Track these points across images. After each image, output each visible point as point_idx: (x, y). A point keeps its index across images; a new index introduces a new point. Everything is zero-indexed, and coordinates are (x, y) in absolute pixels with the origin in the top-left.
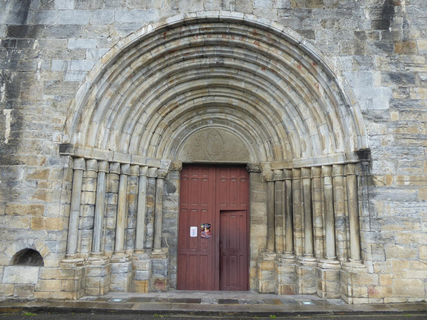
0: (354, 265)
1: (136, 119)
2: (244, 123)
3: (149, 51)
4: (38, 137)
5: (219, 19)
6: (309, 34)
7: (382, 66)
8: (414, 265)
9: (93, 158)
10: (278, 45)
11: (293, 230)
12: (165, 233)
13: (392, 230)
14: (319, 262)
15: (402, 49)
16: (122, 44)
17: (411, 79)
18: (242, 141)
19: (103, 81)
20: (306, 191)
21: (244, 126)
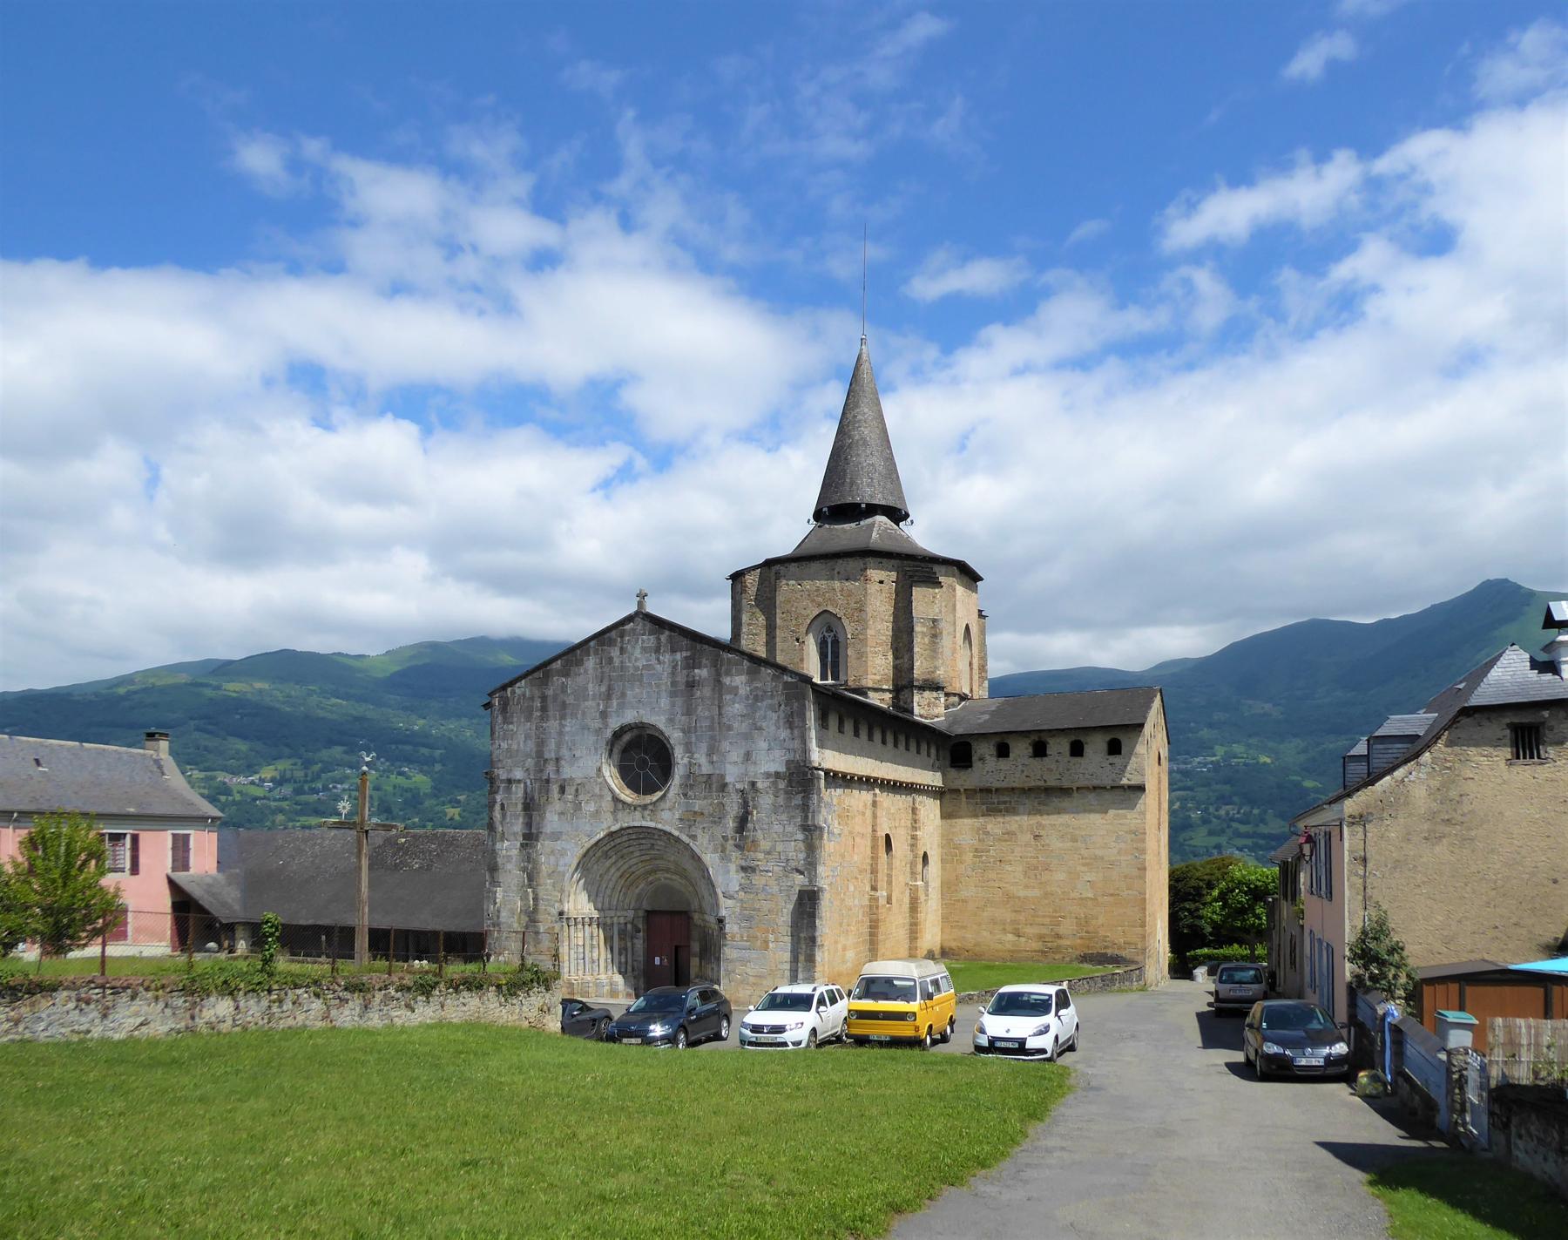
6: (694, 837)
17: (753, 870)
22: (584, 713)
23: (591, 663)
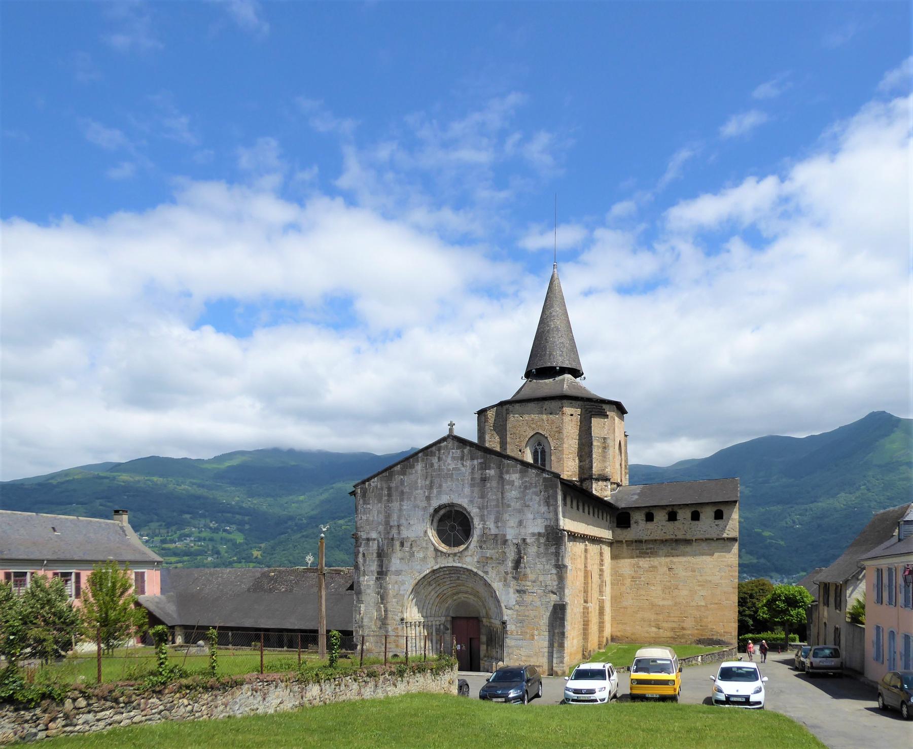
6: (486, 573)
17: (524, 592)
22: (415, 498)
23: (419, 467)
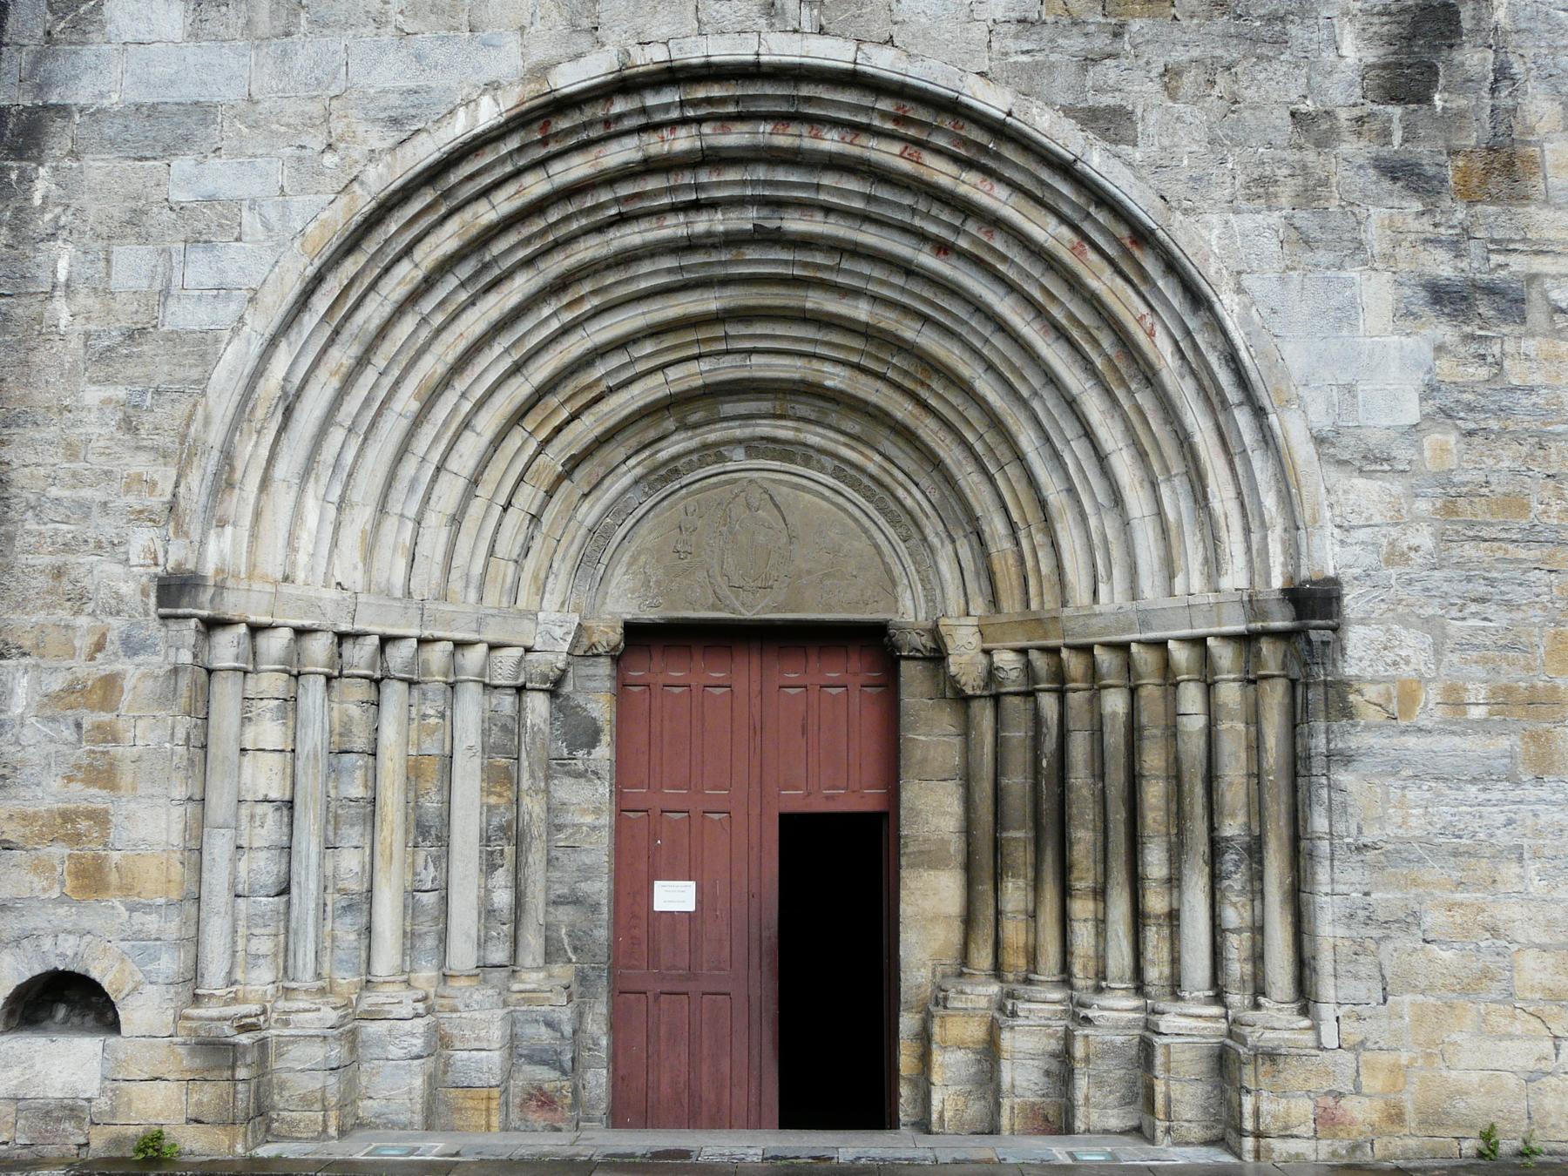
0: (1276, 1022)
1: (435, 457)
2: (871, 460)
3: (485, 193)
4: (74, 552)
5: (758, 64)
6: (1111, 123)
7: (1401, 252)
8: (1493, 1019)
9: (279, 621)
10: (992, 164)
11: (1065, 892)
12: (561, 908)
13: (1414, 891)
14: (1154, 1012)
15: (1483, 182)
16: (380, 177)
17: (1510, 302)
18: (866, 531)
19: (310, 320)
20: (1115, 738)
21: (872, 468)
